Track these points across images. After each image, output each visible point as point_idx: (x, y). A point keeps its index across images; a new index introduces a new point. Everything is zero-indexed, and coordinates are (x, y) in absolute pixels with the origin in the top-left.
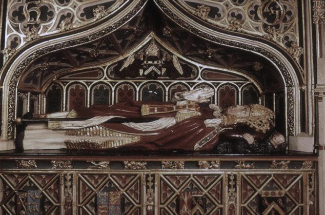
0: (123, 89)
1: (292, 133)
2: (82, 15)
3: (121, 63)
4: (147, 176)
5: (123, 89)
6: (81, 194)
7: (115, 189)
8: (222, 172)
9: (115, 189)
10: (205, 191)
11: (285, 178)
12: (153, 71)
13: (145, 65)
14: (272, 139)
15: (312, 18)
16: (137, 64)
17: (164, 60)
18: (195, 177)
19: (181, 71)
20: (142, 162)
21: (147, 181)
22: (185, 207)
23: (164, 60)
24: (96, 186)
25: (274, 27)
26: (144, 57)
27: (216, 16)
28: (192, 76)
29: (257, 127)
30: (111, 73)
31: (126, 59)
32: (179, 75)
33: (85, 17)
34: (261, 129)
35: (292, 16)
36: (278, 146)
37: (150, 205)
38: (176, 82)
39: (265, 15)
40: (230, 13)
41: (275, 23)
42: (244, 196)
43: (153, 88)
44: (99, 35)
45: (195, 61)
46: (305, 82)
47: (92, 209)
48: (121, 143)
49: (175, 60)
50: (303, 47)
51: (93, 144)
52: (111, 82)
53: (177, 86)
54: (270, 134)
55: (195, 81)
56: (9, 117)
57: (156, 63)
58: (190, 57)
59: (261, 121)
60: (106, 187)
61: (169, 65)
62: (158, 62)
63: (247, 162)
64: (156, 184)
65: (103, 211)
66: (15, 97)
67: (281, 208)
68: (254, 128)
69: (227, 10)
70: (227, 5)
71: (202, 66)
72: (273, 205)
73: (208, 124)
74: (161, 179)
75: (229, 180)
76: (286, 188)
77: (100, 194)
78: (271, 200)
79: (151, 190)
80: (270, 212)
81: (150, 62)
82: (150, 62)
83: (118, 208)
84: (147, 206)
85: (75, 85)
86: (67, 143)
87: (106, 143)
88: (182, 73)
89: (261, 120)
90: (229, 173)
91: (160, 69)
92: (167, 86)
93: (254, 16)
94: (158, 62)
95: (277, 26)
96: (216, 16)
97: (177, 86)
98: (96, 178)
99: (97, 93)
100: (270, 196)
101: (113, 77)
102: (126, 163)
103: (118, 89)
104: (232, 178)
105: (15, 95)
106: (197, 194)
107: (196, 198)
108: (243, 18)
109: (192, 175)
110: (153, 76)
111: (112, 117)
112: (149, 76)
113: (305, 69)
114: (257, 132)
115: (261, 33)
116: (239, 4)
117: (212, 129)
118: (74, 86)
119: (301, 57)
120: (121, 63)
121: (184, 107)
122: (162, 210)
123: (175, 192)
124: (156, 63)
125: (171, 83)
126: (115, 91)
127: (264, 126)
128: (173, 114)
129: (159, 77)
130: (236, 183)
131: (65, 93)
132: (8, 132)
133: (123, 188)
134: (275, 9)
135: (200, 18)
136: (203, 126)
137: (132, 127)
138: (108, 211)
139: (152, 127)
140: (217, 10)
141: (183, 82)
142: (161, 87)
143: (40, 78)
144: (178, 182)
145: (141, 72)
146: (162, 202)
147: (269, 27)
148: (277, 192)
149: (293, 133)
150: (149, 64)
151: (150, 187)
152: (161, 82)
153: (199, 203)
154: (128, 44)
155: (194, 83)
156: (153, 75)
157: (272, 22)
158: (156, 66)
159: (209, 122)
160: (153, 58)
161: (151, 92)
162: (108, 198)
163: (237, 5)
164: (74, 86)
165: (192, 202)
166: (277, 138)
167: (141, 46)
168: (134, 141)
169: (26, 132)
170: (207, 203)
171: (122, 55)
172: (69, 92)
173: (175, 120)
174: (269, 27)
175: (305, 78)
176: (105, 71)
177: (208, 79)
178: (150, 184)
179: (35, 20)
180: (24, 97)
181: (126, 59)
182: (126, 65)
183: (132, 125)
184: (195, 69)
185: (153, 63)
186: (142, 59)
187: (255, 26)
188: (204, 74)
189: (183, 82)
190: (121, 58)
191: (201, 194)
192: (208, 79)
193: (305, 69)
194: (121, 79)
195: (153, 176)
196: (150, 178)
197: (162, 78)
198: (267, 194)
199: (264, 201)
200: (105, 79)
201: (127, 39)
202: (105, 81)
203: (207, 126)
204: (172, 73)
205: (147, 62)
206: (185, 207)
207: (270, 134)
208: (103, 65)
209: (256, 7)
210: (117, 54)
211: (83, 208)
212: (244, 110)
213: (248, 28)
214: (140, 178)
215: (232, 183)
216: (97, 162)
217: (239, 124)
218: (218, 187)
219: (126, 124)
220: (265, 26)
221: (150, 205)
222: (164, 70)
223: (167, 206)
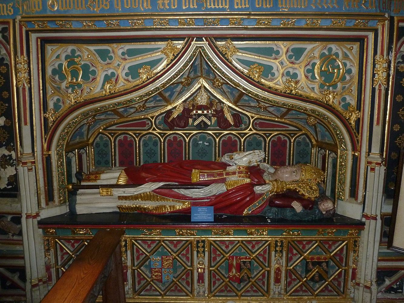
0: (172, 140)
1: (341, 198)
2: (127, 74)
5: (172, 140)
6: (135, 258)
11: (330, 243)
12: (202, 121)
13: (195, 115)
14: (320, 204)
15: (373, 81)
16: (186, 113)
17: (214, 109)
18: (244, 242)
21: (198, 247)
24: (149, 250)
25: (331, 88)
26: (193, 106)
27: (270, 75)
28: (243, 126)
30: (160, 125)
31: (175, 107)
32: (230, 125)
33: (130, 78)
34: (311, 197)
35: (351, 74)
36: (326, 212)
37: (201, 268)
38: (226, 132)
39: (322, 73)
40: (285, 74)
43: (203, 138)
44: (145, 96)
45: (247, 111)
46: (358, 148)
47: (147, 271)
48: (172, 208)
49: (225, 110)
50: (360, 111)
52: (159, 133)
53: (228, 136)
56: (59, 182)
57: (205, 112)
58: (242, 107)
60: (159, 251)
61: (219, 114)
62: (208, 112)
65: (157, 274)
66: (63, 160)
68: (303, 195)
69: (282, 68)
70: (282, 63)
71: (253, 115)
73: (258, 191)
74: (211, 244)
80: (314, 275)
81: (200, 112)
82: (200, 112)
84: (198, 269)
85: (123, 136)
86: (119, 208)
87: (157, 208)
91: (210, 120)
92: (217, 137)
93: (310, 74)
94: (208, 112)
97: (228, 136)
98: (149, 243)
99: (145, 145)
103: (167, 139)
105: (63, 158)
108: (299, 78)
109: (240, 241)
110: (203, 126)
111: (161, 184)
112: (199, 127)
113: (360, 134)
114: (304, 199)
116: (296, 61)
117: (261, 195)
118: (122, 137)
119: (358, 121)
120: (170, 112)
121: (234, 173)
122: (212, 271)
123: (224, 256)
125: (222, 133)
128: (223, 181)
130: (282, 249)
133: (175, 253)
135: (253, 80)
136: (253, 192)
137: (183, 193)
138: (162, 274)
139: (202, 194)
140: (271, 68)
141: (233, 132)
142: (211, 137)
144: (227, 247)
145: (190, 120)
149: (343, 198)
150: (199, 114)
153: (247, 267)
154: (176, 94)
155: (246, 134)
156: (203, 126)
158: (205, 116)
159: (258, 189)
160: (201, 107)
161: (201, 142)
163: (292, 63)
164: (122, 137)
165: (240, 266)
166: (326, 205)
167: (190, 95)
168: (184, 207)
169: (78, 197)
170: (254, 266)
171: (170, 104)
172: (117, 143)
173: (225, 187)
175: (360, 144)
177: (260, 129)
178: (201, 250)
179: (77, 80)
180: (72, 155)
182: (175, 115)
183: (183, 192)
184: (247, 118)
185: (203, 112)
186: (191, 108)
189: (233, 132)
190: (169, 107)
192: (260, 129)
193: (360, 134)
194: (171, 130)
196: (201, 244)
197: (212, 128)
199: (309, 265)
200: (154, 129)
202: (154, 132)
203: (256, 192)
204: (223, 123)
205: (197, 112)
208: (151, 115)
209: (314, 64)
210: (165, 104)
211: (138, 270)
212: (294, 172)
217: (289, 190)
218: (265, 252)
219: (176, 190)
220: (322, 86)
221: (201, 268)
222: (214, 120)
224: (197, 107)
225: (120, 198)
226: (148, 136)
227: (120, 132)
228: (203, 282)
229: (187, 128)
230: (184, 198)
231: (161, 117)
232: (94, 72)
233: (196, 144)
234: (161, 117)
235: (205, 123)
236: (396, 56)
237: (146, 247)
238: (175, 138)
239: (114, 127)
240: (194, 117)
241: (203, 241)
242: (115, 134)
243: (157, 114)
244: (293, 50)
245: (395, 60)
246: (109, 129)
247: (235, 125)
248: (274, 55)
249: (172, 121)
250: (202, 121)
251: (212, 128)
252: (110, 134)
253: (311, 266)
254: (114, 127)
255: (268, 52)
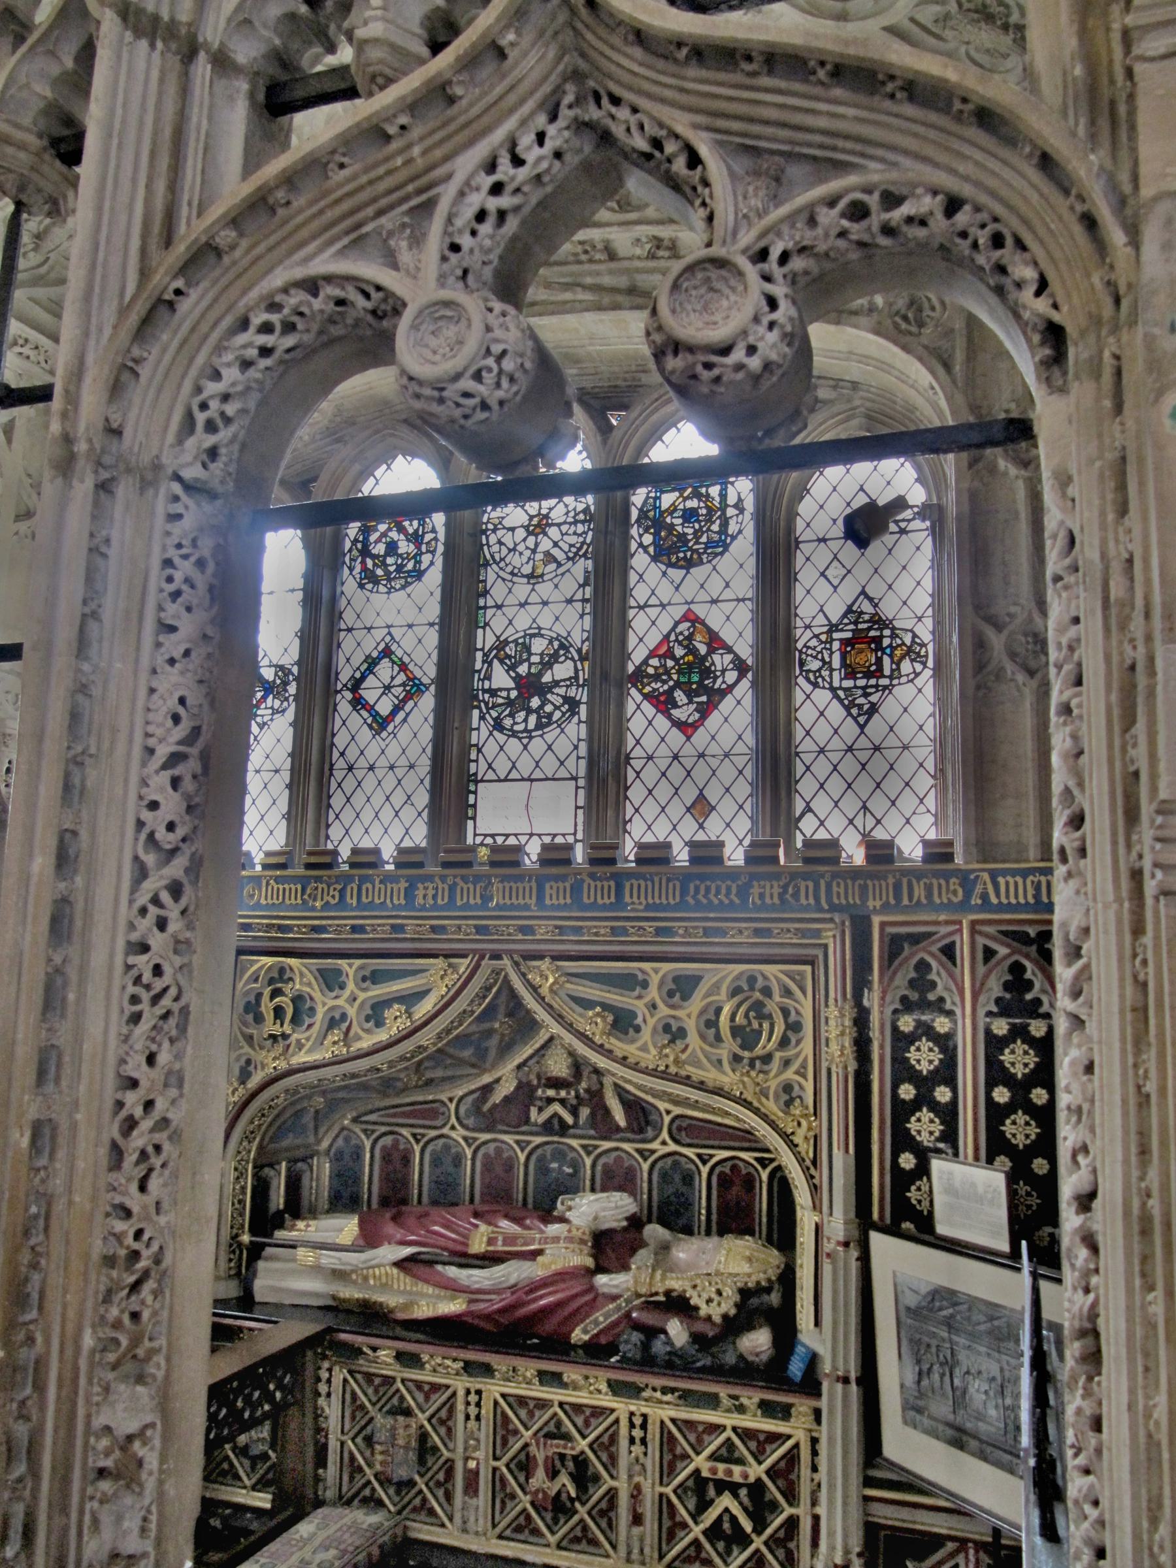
3: (487, 1089)
4: (468, 1392)
7: (408, 1412)
8: (622, 1407)
9: (408, 1412)
10: (583, 1444)
12: (556, 1115)
13: (541, 1099)
16: (524, 1094)
19: (619, 1116)
20: (455, 1360)
21: (468, 1403)
22: (540, 1473)
23: (584, 1085)
25: (758, 1063)
26: (539, 1077)
28: (650, 1133)
29: (703, 1306)
30: (468, 1114)
31: (498, 1081)
32: (618, 1129)
38: (607, 1145)
39: (736, 1031)
40: (660, 1029)
41: (759, 1051)
42: (667, 1470)
43: (559, 1155)
51: (381, 1304)
52: (465, 1139)
54: (735, 1326)
55: (655, 1145)
57: (563, 1094)
59: (719, 1293)
63: (665, 1390)
64: (483, 1412)
67: (745, 1509)
68: (697, 1308)
72: (726, 1501)
75: (632, 1425)
76: (760, 1463)
77: (379, 1419)
78: (723, 1486)
79: (472, 1424)
81: (551, 1093)
82: (551, 1093)
83: (412, 1456)
88: (622, 1123)
89: (720, 1286)
90: (633, 1408)
91: (574, 1112)
95: (767, 1058)
96: (631, 1030)
99: (436, 1162)
100: (720, 1475)
101: (470, 1122)
102: (425, 1358)
104: (638, 1421)
106: (565, 1447)
107: (562, 1457)
108: (688, 1040)
111: (408, 1251)
115: (728, 1079)
118: (388, 1140)
120: (487, 1089)
121: (556, 1239)
124: (563, 1094)
126: (473, 1159)
127: (719, 1304)
129: (572, 1131)
131: (368, 1156)
132: (230, 1260)
134: (761, 1017)
136: (592, 1288)
140: (634, 1015)
143: (311, 1125)
145: (533, 1112)
146: (498, 1452)
147: (746, 1061)
148: (737, 1470)
151: (472, 1417)
152: (574, 1143)
155: (653, 1152)
156: (556, 1127)
157: (751, 1049)
158: (563, 1102)
159: (602, 1280)
160: (556, 1083)
162: (393, 1428)
163: (672, 1007)
164: (388, 1140)
165: (554, 1466)
174: (746, 1061)
176: (452, 1107)
178: (473, 1411)
181: (498, 1081)
182: (497, 1097)
183: (452, 1271)
186: (535, 1082)
187: (714, 1058)
188: (680, 1129)
189: (626, 1146)
190: (487, 1079)
191: (573, 1448)
192: (688, 1141)
195: (479, 1392)
197: (579, 1132)
198: (714, 1471)
200: (453, 1128)
201: (484, 1045)
202: (453, 1134)
206: (540, 1473)
207: (735, 1326)
208: (450, 1095)
209: (718, 1011)
213: (697, 1064)
214: (454, 1394)
215: (637, 1433)
216: (374, 1349)
219: (439, 1267)
220: (737, 1059)
222: (585, 1112)
223: (507, 1466)
224: (549, 1079)
225: (339, 1275)
226: (441, 1141)
227: (383, 1129)
228: (476, 1493)
229: (524, 1128)
230: (454, 1288)
231: (470, 1099)
232: (312, 1010)
233: (543, 1169)
234: (470, 1099)
235: (561, 1121)
236: (883, 998)
237: (370, 1391)
238: (499, 1151)
239: (373, 1117)
240: (539, 1103)
241: (479, 1392)
242: (373, 1131)
243: (461, 1093)
244: (676, 979)
245: (882, 1005)
246: (364, 1119)
247: (630, 1128)
248: (638, 990)
249: (490, 1110)
250: (556, 1115)
251: (579, 1132)
252: (365, 1131)
253: (711, 1492)
254: (373, 1117)
255: (628, 982)
